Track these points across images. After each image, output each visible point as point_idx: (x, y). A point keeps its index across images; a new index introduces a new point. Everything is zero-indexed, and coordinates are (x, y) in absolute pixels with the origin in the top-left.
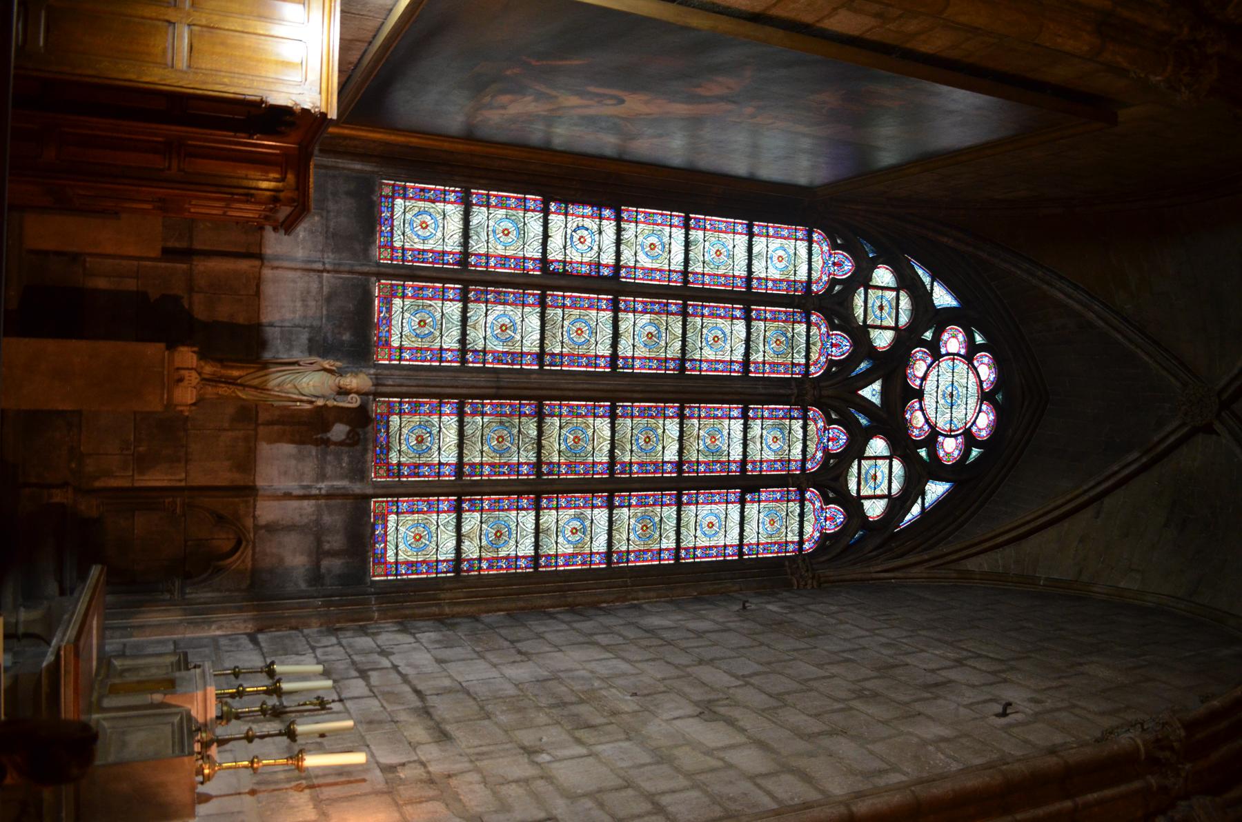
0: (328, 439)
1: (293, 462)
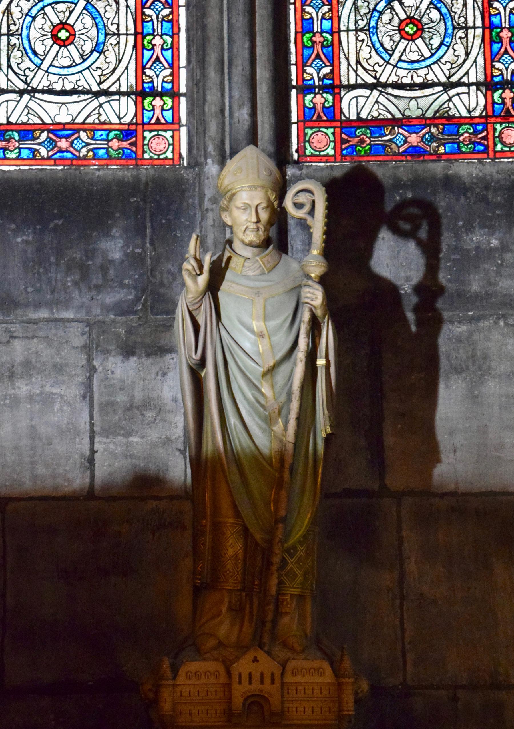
0: (418, 289)
1: (492, 387)
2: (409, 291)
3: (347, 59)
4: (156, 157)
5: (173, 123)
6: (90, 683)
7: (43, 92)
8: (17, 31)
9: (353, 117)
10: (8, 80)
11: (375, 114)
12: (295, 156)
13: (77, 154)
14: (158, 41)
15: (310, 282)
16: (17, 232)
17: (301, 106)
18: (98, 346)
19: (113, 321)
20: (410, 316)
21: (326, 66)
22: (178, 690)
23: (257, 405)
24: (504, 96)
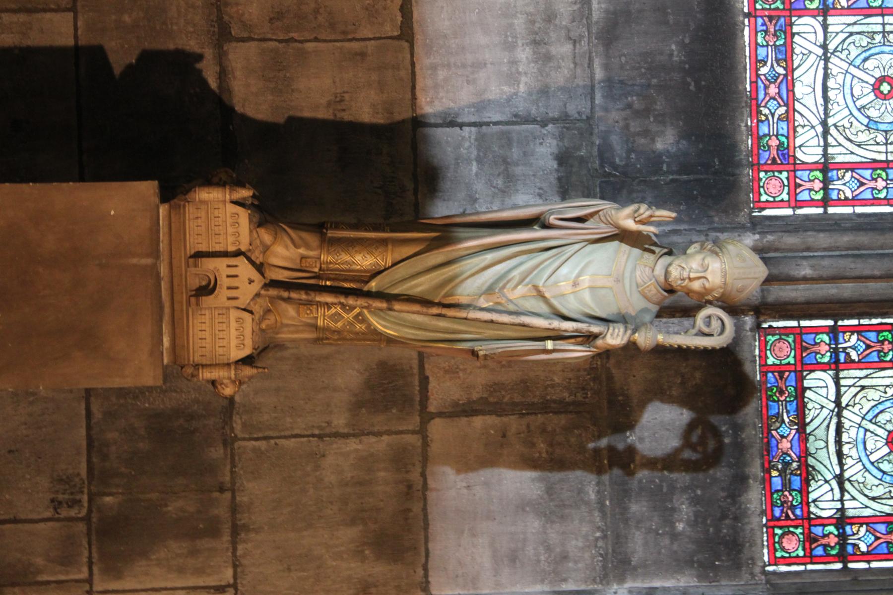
0: (631, 451)
1: (534, 524)
2: (629, 440)
3: (866, 377)
4: (761, 184)
6: (231, 127)
7: (826, 68)
8: (888, 41)
9: (806, 384)
10: (837, 33)
11: (810, 406)
12: (765, 325)
13: (763, 104)
14: (881, 184)
15: (629, 332)
16: (682, 45)
17: (817, 330)
18: (568, 128)
19: (593, 143)
20: (604, 442)
21: (859, 355)
22: (221, 205)
23: (505, 281)
24: (831, 536)
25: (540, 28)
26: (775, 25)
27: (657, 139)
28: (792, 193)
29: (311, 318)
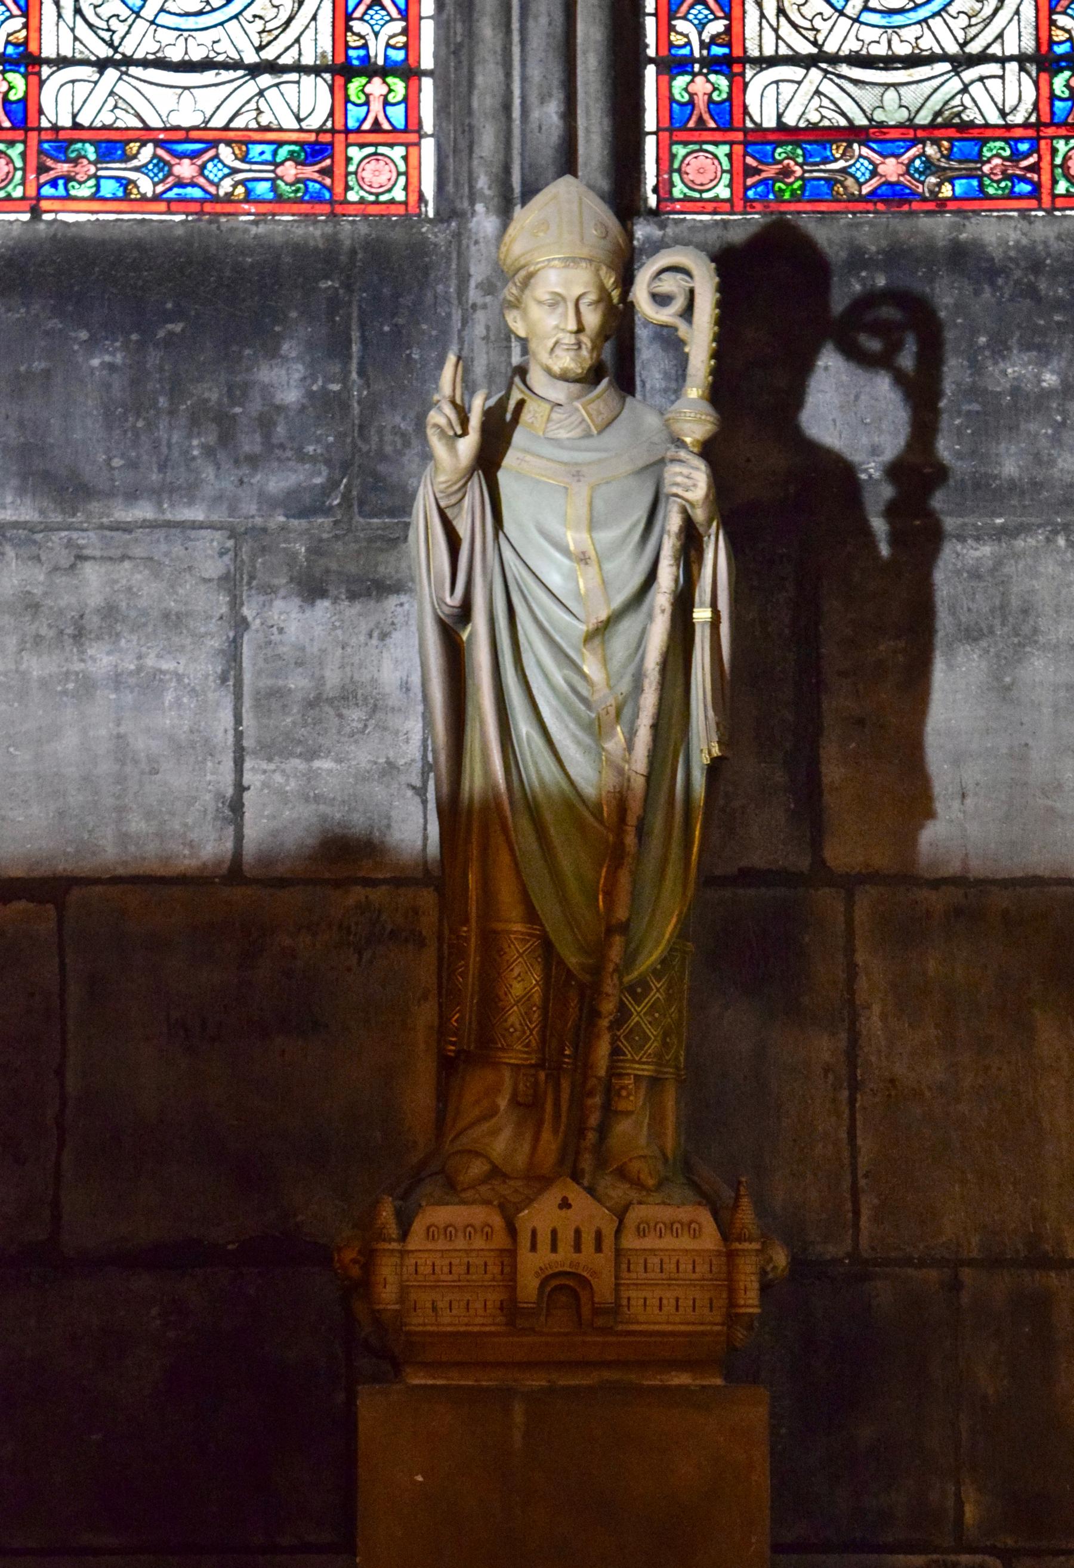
0: (895, 471)
1: (1039, 669)
2: (877, 475)
4: (372, 198)
5: (406, 130)
6: (230, 1247)
7: (145, 63)
9: (770, 122)
10: (76, 39)
11: (814, 118)
12: (652, 201)
13: (212, 190)
15: (683, 454)
16: (92, 345)
17: (666, 99)
18: (252, 578)
19: (283, 528)
20: (879, 525)
21: (716, 18)
22: (410, 1261)
23: (573, 698)
25: (50, 626)
26: (57, 160)
27: (277, 401)
28: (389, 138)
29: (637, 1088)
